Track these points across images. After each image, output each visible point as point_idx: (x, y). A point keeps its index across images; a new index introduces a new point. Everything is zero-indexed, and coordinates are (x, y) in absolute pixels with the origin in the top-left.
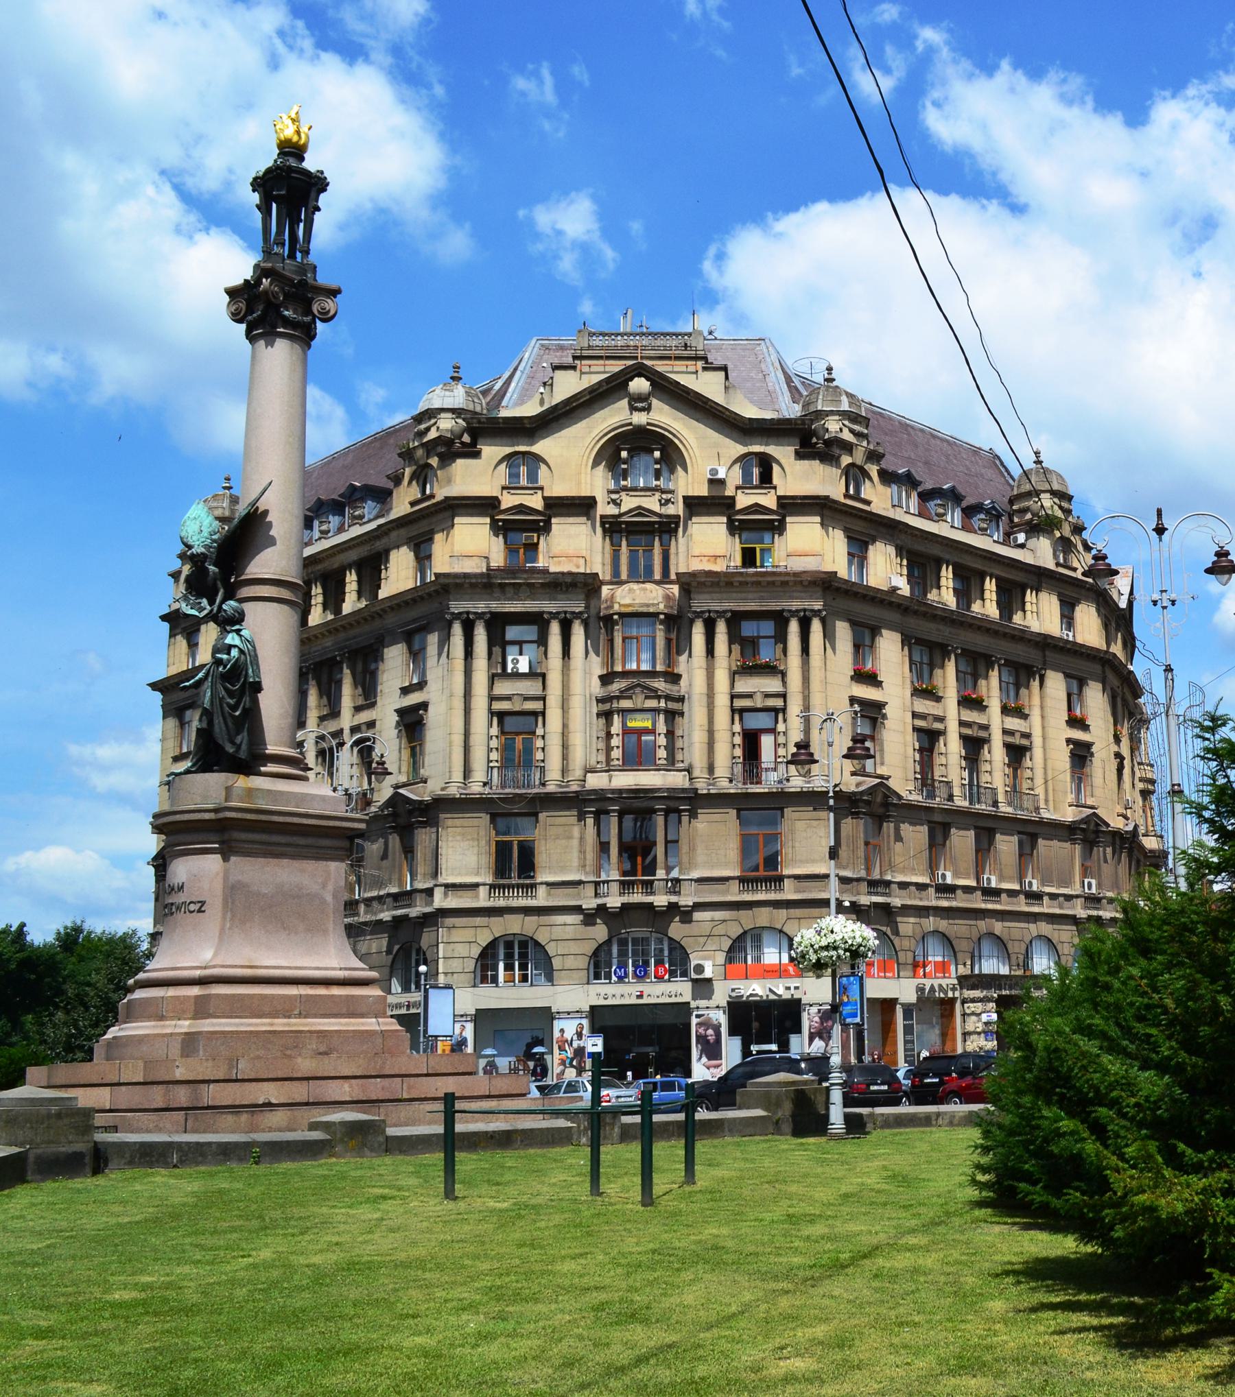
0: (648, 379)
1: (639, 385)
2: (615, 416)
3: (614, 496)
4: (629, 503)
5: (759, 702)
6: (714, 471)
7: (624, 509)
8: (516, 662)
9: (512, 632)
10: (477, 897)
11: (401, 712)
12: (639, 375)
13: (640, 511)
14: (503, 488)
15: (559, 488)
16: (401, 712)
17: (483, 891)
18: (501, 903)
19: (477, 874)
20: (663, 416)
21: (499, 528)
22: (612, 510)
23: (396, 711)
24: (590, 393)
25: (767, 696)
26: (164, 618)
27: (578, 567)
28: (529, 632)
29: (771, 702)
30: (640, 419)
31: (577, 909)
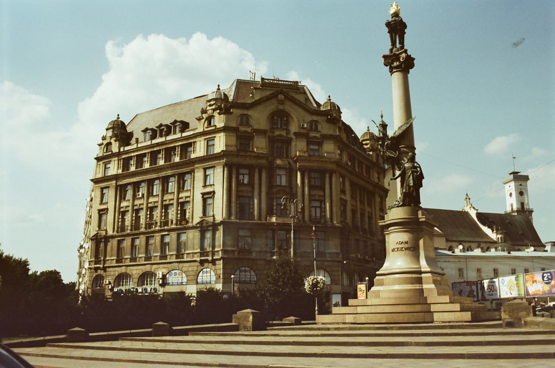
0: (283, 95)
1: (281, 97)
2: (272, 106)
3: (273, 131)
4: (277, 133)
5: (317, 198)
6: (303, 125)
7: (275, 134)
8: (243, 180)
9: (242, 171)
10: (234, 254)
11: (203, 194)
12: (281, 93)
13: (280, 135)
14: (239, 125)
15: (256, 127)
16: (203, 194)
17: (236, 253)
18: (242, 257)
19: (234, 247)
20: (289, 107)
21: (238, 138)
22: (271, 134)
23: (201, 194)
24: (267, 97)
25: (319, 196)
26: (96, 159)
27: (264, 151)
28: (246, 171)
29: (320, 198)
30: (281, 107)
31: (265, 260)
